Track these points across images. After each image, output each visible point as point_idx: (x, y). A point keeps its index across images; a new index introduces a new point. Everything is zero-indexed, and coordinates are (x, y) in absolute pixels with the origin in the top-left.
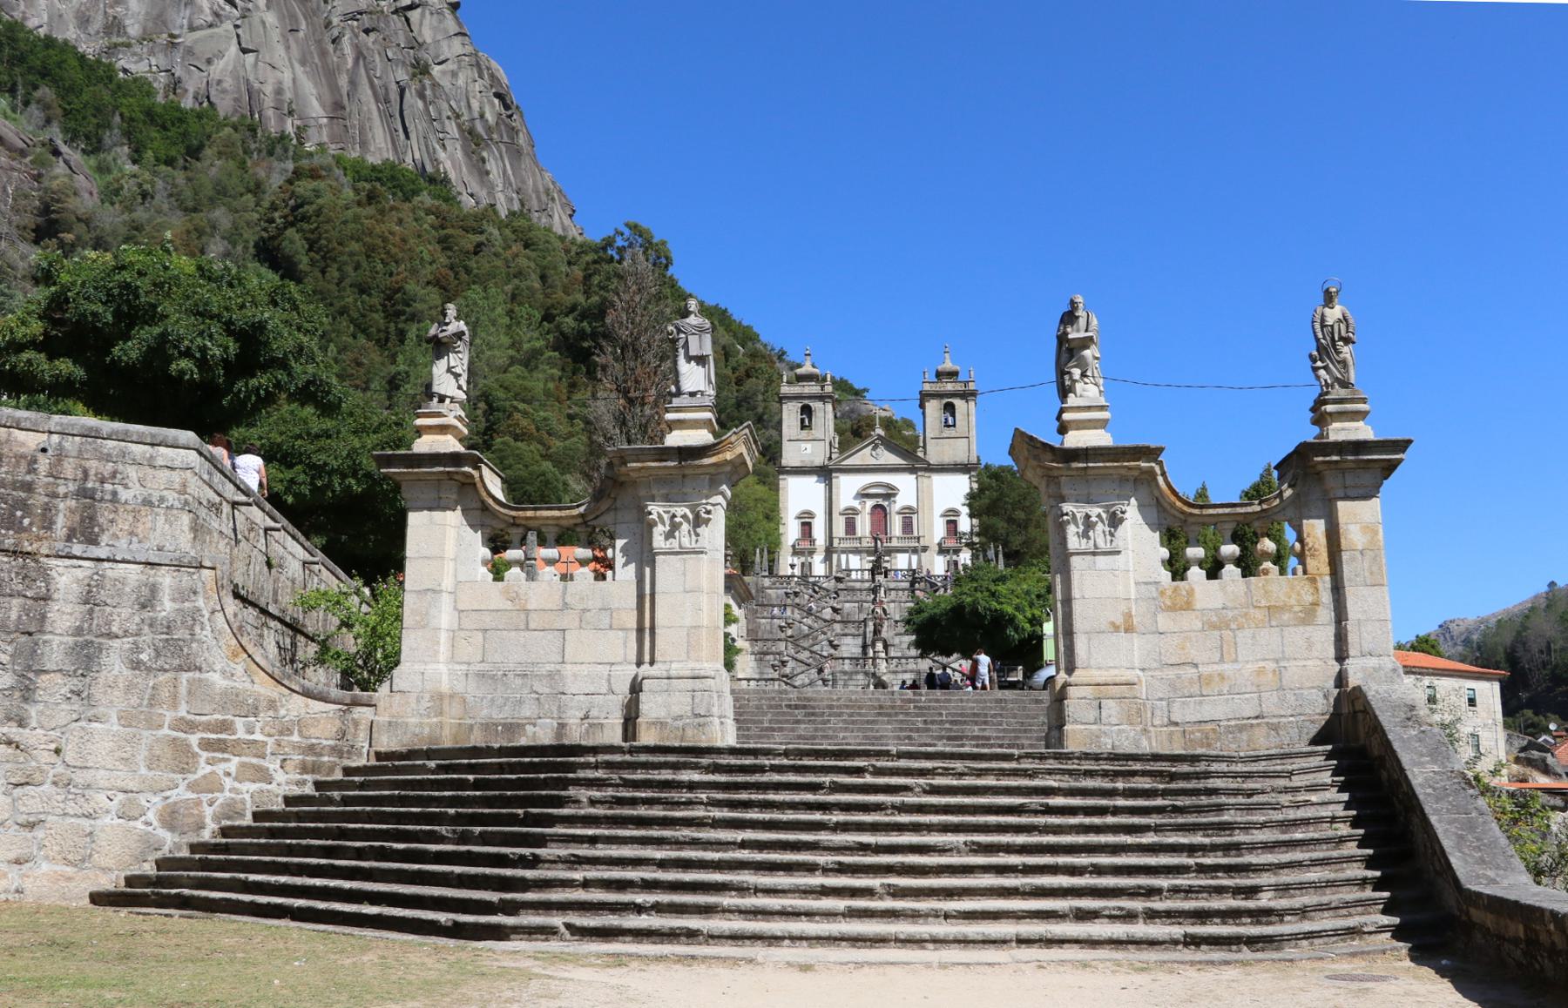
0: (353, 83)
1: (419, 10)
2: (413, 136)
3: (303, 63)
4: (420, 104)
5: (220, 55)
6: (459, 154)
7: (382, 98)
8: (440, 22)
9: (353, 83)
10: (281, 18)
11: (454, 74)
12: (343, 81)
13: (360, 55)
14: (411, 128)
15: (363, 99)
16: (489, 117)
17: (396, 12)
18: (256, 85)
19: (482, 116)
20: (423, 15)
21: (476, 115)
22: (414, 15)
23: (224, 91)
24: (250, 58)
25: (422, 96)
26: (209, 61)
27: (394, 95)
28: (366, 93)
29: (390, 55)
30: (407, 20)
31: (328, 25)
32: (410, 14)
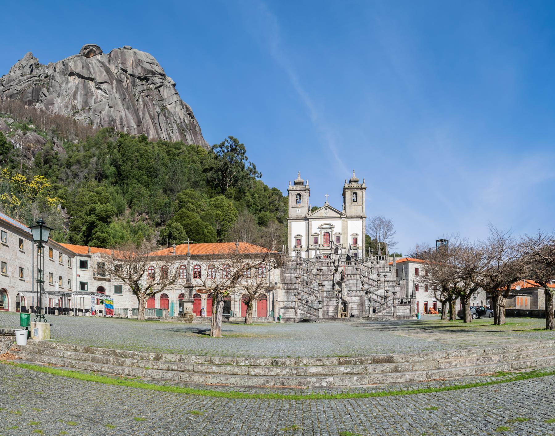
0: (144, 114)
1: (162, 87)
2: (163, 129)
3: (128, 109)
4: (164, 118)
5: (103, 110)
6: (178, 134)
7: (152, 118)
8: (169, 90)
9: (144, 114)
10: (121, 95)
11: (175, 108)
12: (141, 114)
13: (145, 105)
14: (162, 127)
15: (147, 119)
16: (186, 121)
17: (155, 89)
18: (115, 118)
19: (184, 121)
20: (164, 89)
21: (182, 121)
22: (161, 89)
23: (105, 121)
24: (112, 109)
25: (165, 116)
26: (100, 113)
27: (156, 117)
28: (147, 116)
29: (154, 103)
31: (135, 95)
32: (159, 89)
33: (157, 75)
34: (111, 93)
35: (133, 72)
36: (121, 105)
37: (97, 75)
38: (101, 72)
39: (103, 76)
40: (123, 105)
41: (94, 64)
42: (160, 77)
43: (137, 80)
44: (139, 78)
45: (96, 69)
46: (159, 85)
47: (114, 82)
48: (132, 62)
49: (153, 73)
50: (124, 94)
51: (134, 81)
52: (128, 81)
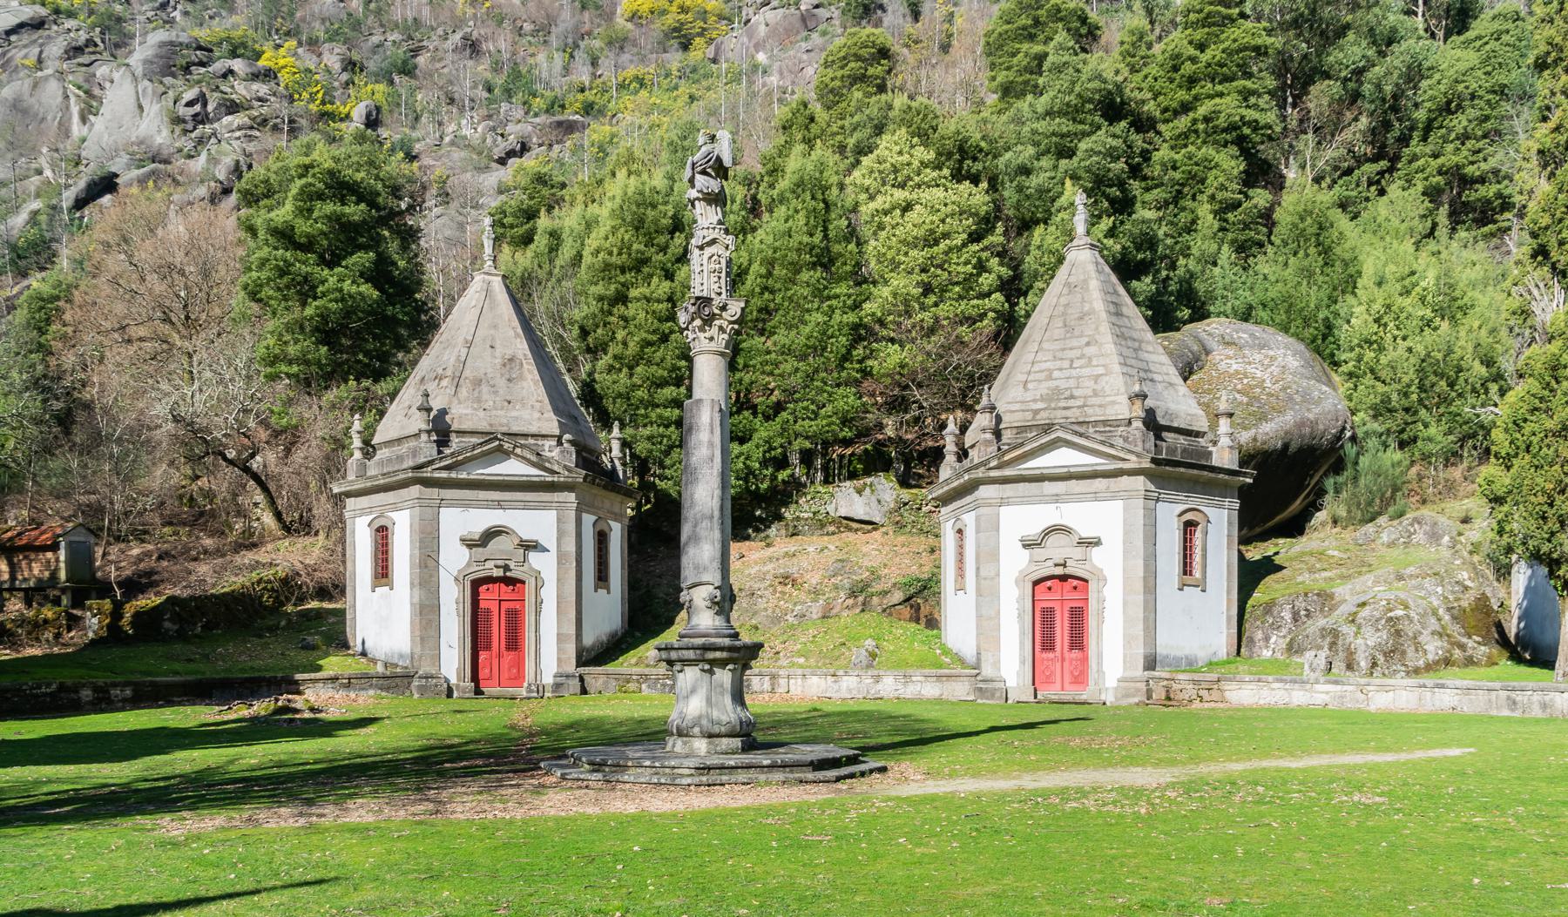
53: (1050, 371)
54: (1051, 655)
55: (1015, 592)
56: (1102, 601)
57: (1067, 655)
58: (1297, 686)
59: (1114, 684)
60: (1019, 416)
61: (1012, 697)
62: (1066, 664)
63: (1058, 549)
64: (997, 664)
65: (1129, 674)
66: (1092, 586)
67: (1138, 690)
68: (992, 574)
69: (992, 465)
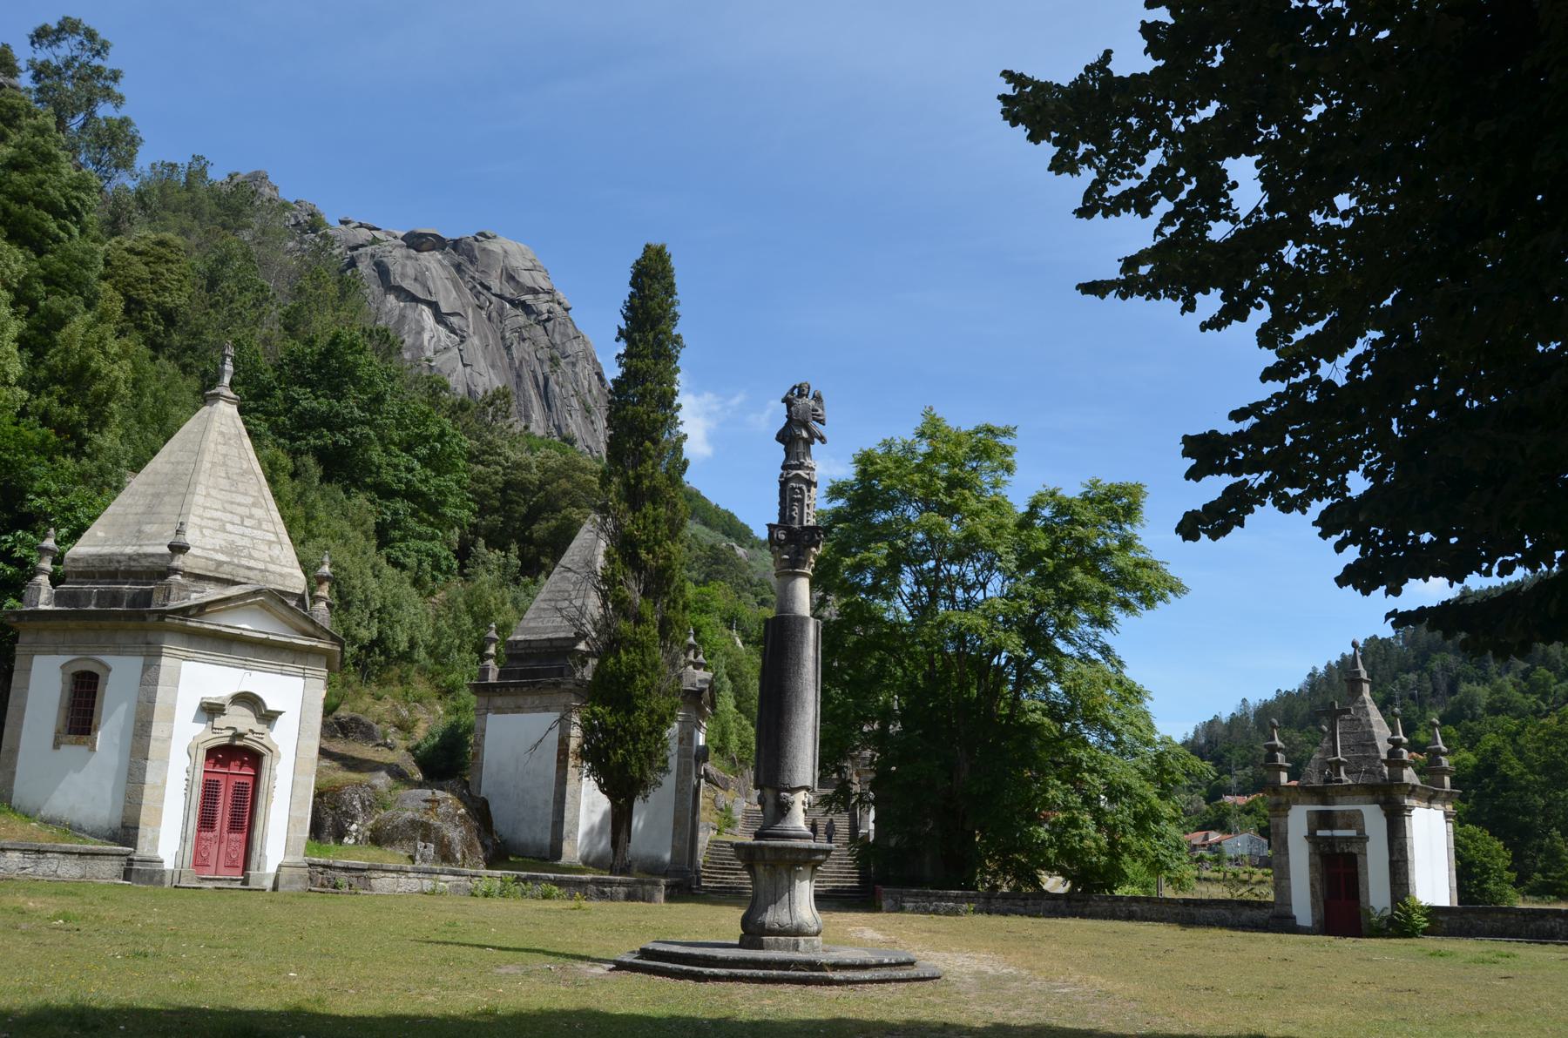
3: (493, 366)
6: (580, 420)
10: (481, 339)
18: (473, 387)
24: (468, 370)
30: (545, 328)
32: (547, 324)
33: (541, 295)
34: (465, 334)
35: (501, 289)
36: (482, 363)
37: (441, 296)
38: (446, 289)
39: (452, 299)
40: (485, 359)
41: (433, 270)
42: (547, 297)
43: (508, 306)
44: (511, 302)
45: (439, 283)
46: (545, 316)
47: (470, 311)
48: (499, 271)
49: (534, 291)
50: (486, 337)
51: (502, 308)
52: (492, 306)
53: (223, 523)
54: (210, 835)
55: (186, 762)
56: (272, 778)
57: (225, 835)
58: (427, 876)
59: (274, 870)
60: (202, 563)
61: (168, 879)
62: (224, 846)
63: (242, 720)
64: (154, 843)
65: (290, 860)
66: (266, 762)
67: (301, 877)
68: (165, 735)
69: (191, 613)
